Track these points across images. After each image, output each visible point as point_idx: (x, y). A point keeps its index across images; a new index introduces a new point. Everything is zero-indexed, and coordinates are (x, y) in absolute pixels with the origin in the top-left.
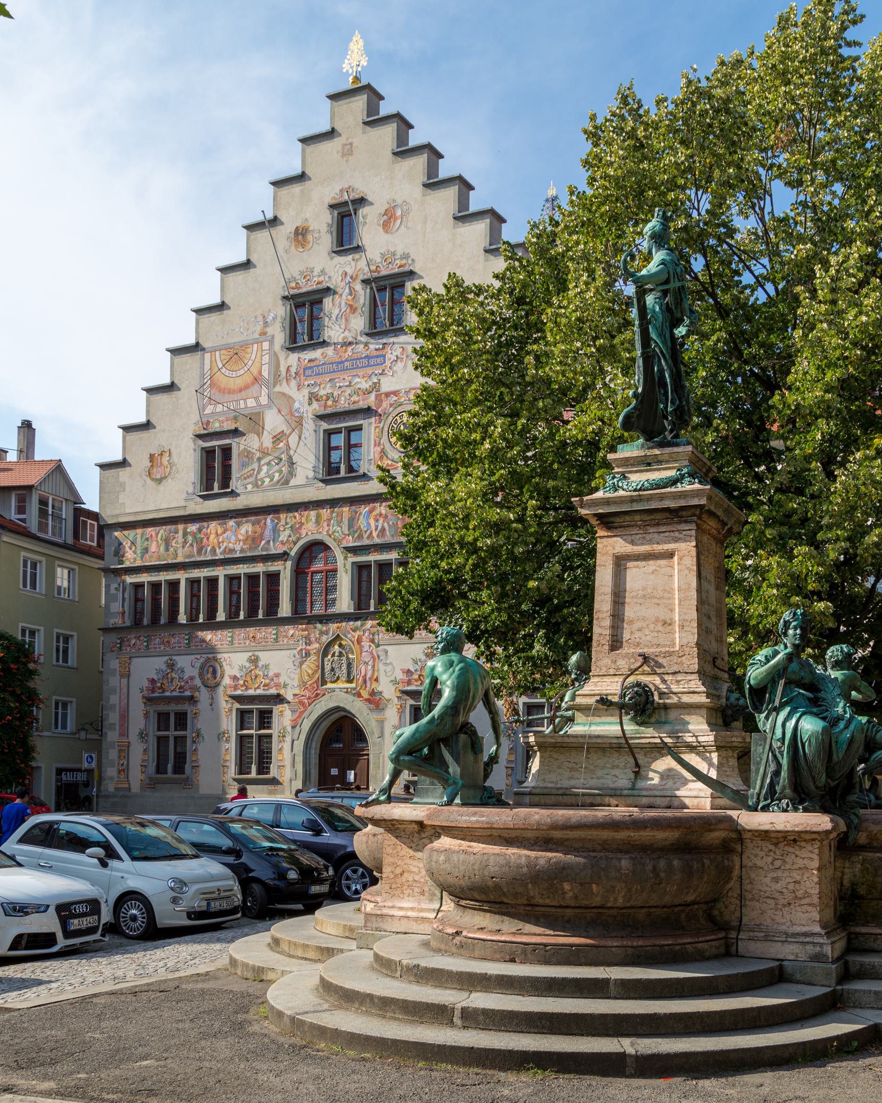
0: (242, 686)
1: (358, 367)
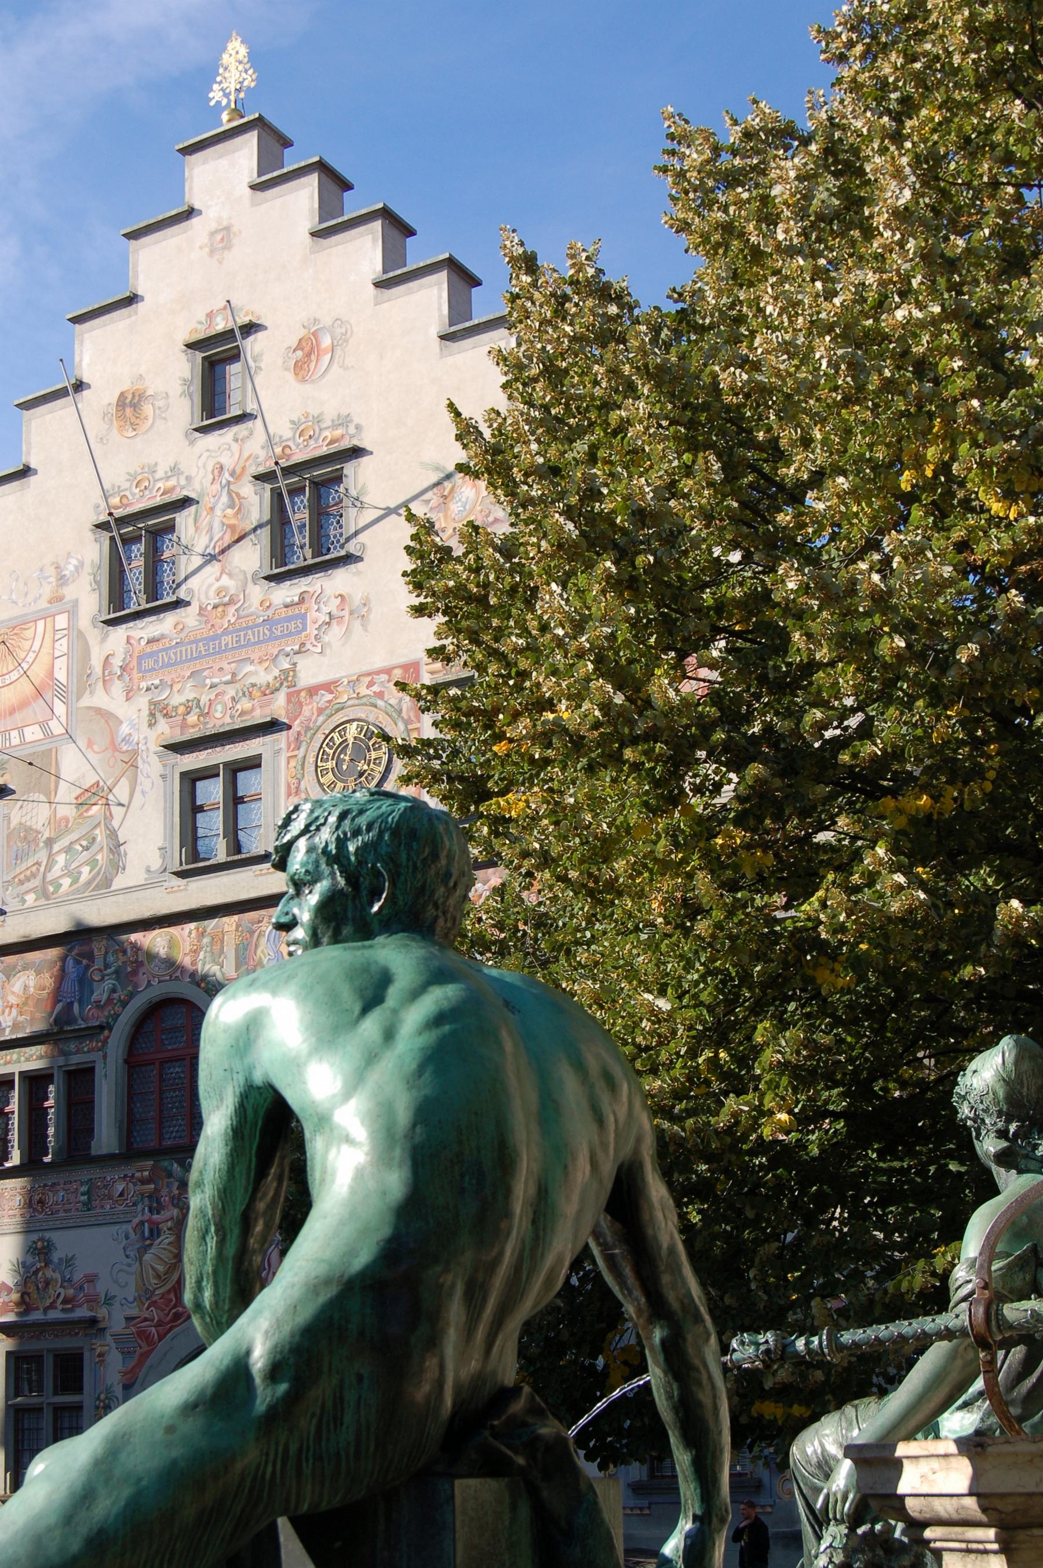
1: (249, 644)
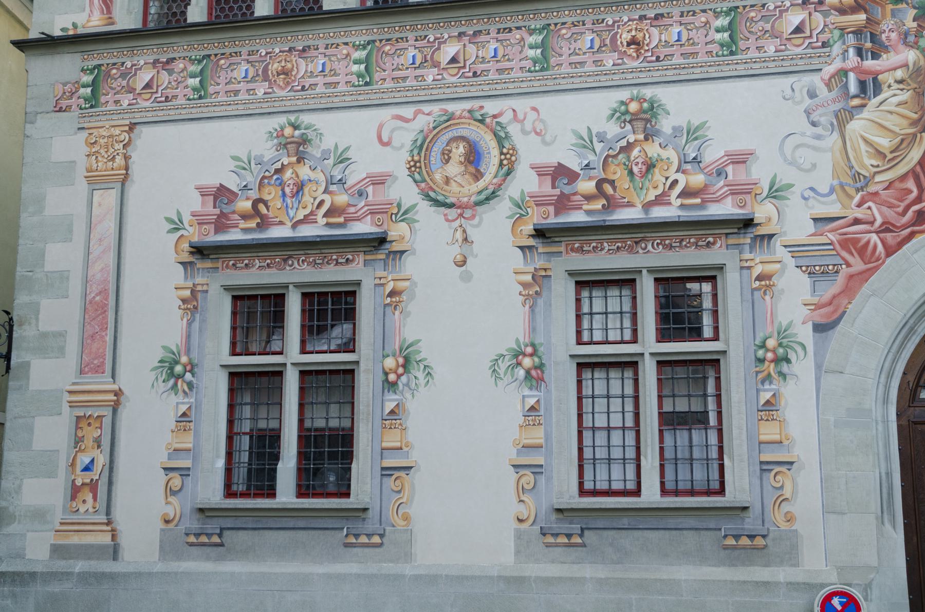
0: (589, 198)
